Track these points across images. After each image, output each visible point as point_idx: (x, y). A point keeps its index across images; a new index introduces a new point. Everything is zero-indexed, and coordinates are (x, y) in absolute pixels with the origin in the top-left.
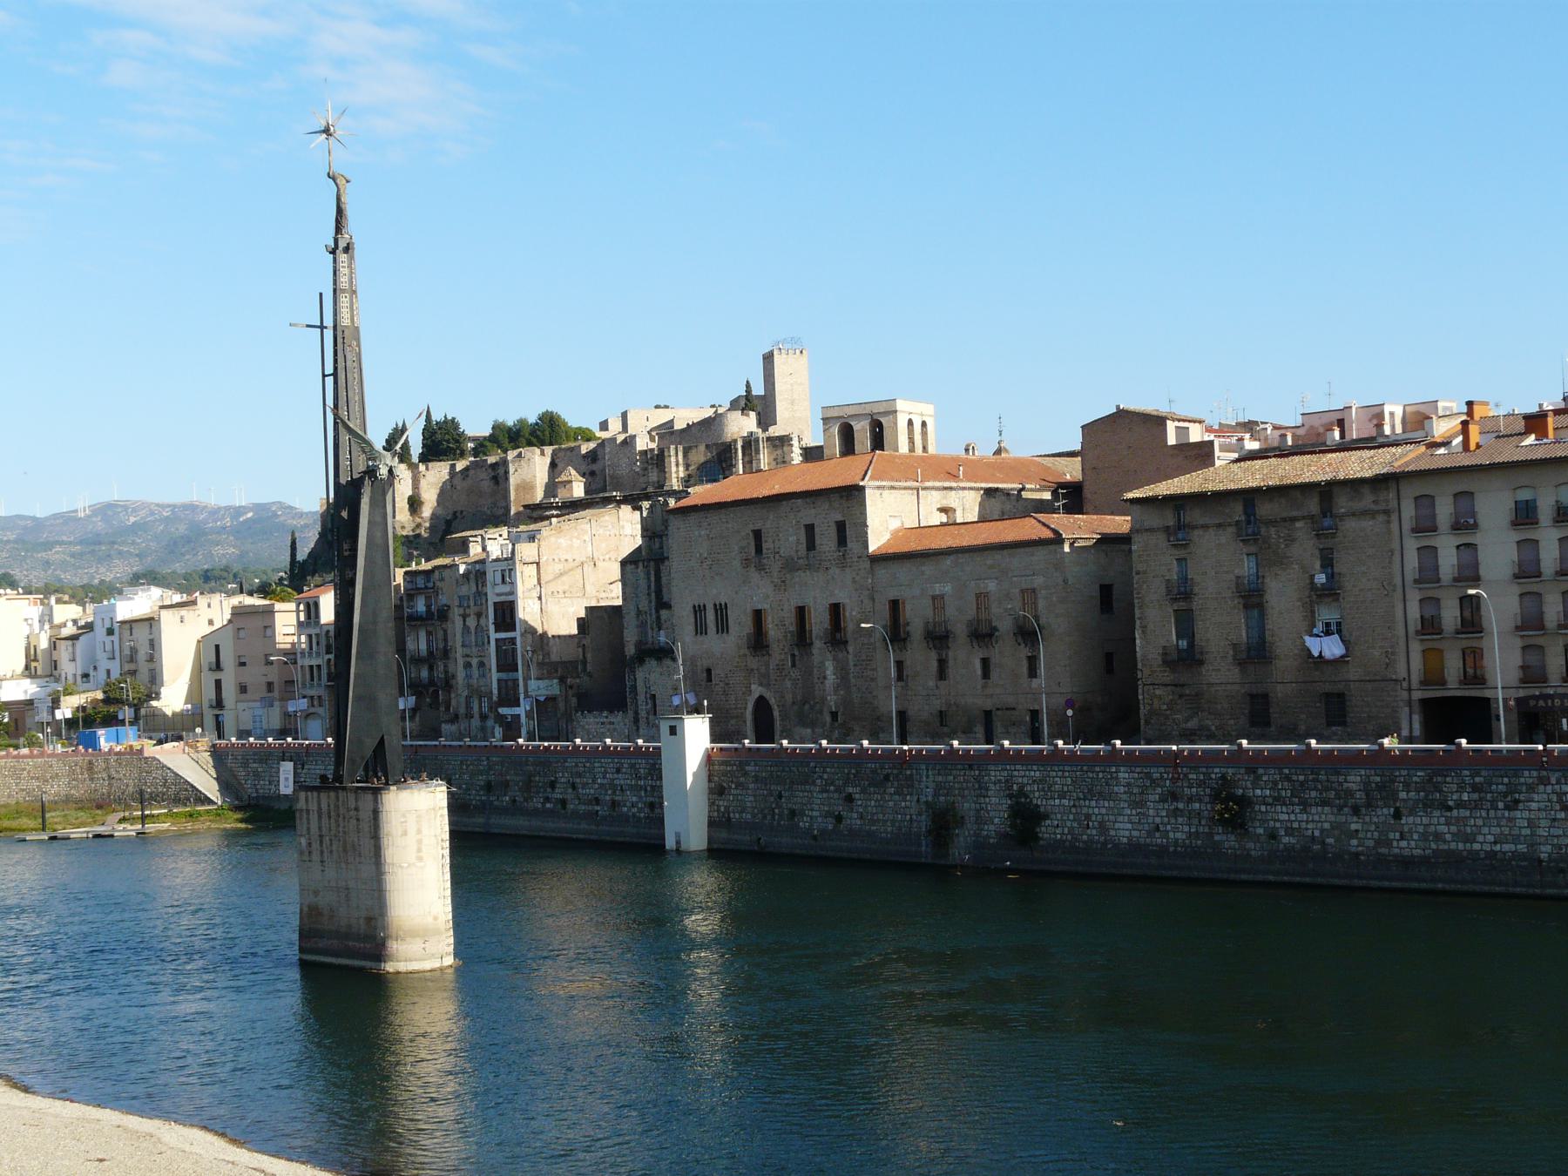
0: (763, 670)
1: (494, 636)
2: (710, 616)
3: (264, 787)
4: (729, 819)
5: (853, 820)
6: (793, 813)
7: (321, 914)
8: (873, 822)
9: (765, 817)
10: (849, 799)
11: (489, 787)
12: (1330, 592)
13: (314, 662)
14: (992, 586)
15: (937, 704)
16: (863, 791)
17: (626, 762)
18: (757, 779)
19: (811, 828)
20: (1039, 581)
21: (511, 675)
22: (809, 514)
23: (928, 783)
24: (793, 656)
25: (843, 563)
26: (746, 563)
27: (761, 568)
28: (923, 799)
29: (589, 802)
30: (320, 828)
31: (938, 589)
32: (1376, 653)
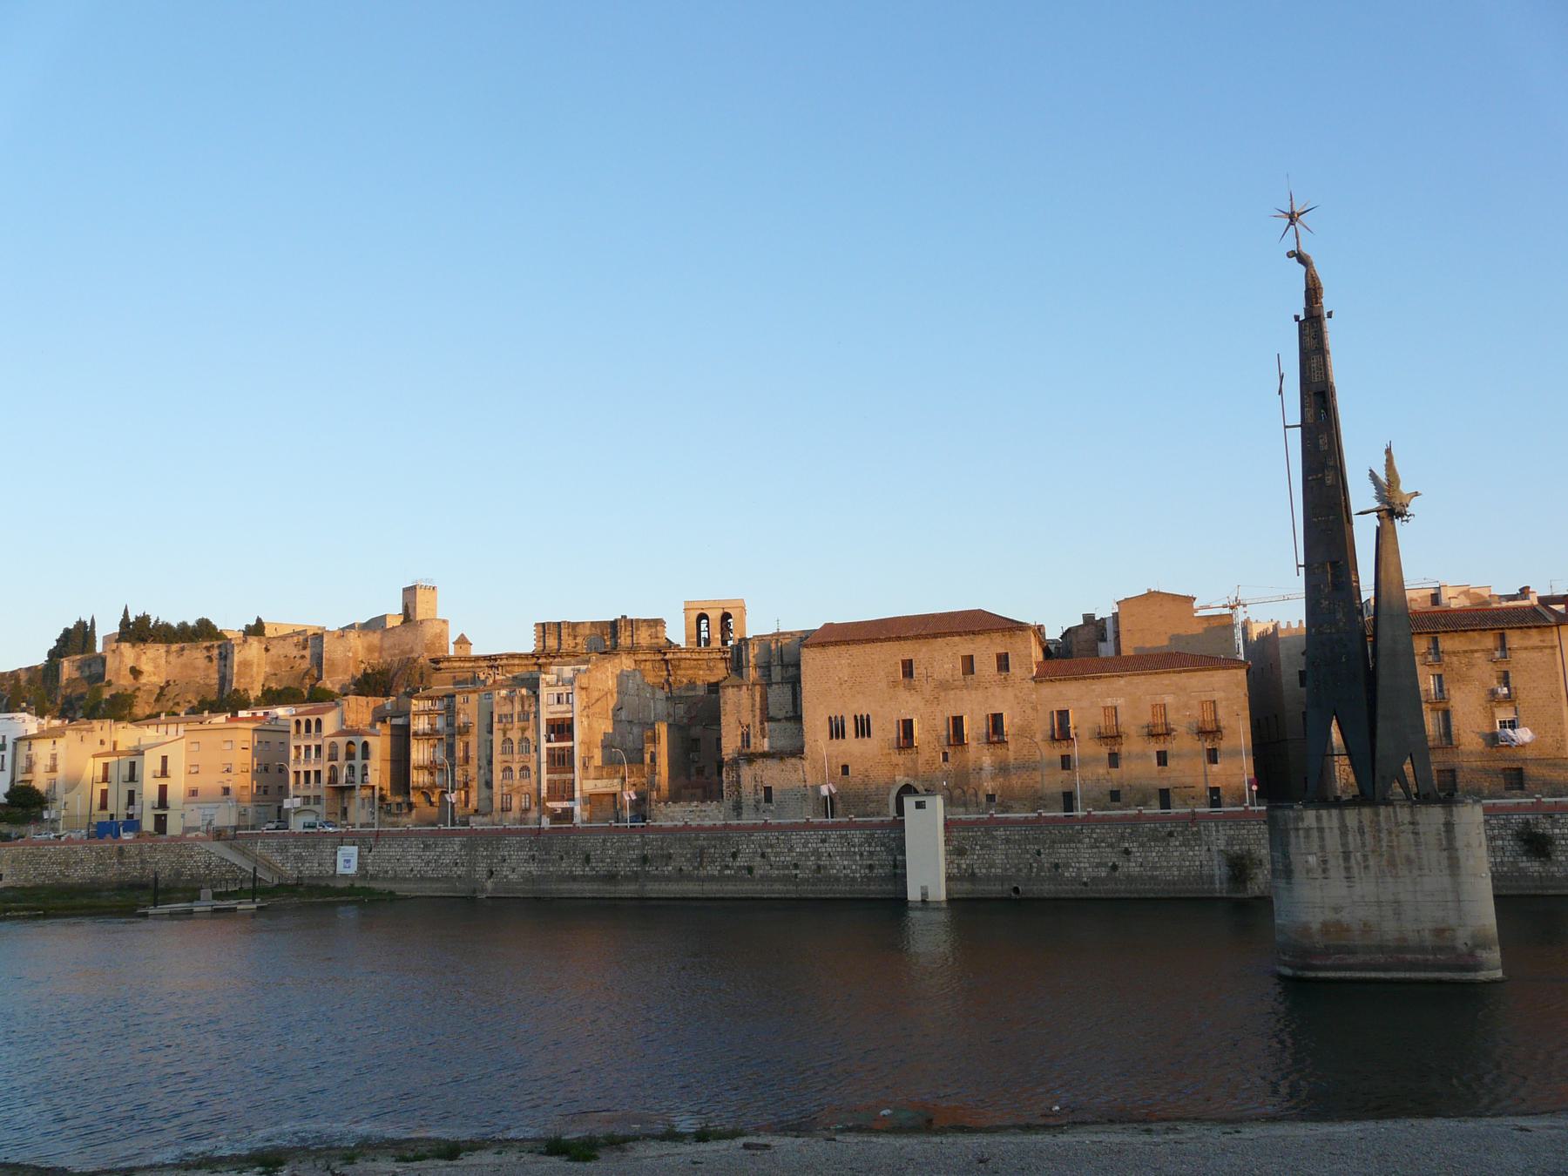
0: (909, 765)
1: (544, 745)
2: (850, 727)
3: (311, 868)
4: (973, 874)
5: (1133, 868)
6: (1057, 866)
7: (1348, 930)
8: (1154, 868)
9: (1020, 870)
10: (1127, 852)
11: (644, 859)
12: (1509, 699)
13: (312, 768)
14: (1169, 699)
15: (1109, 786)
16: (1142, 845)
17: (834, 834)
18: (1007, 841)
19: (1079, 876)
20: (1217, 696)
21: (570, 776)
22: (965, 646)
23: (1219, 838)
24: (945, 754)
25: (1005, 684)
26: (895, 684)
27: (910, 688)
28: (1214, 848)
29: (787, 868)
30: (1345, 844)
31: (1109, 702)
32: (1549, 740)
